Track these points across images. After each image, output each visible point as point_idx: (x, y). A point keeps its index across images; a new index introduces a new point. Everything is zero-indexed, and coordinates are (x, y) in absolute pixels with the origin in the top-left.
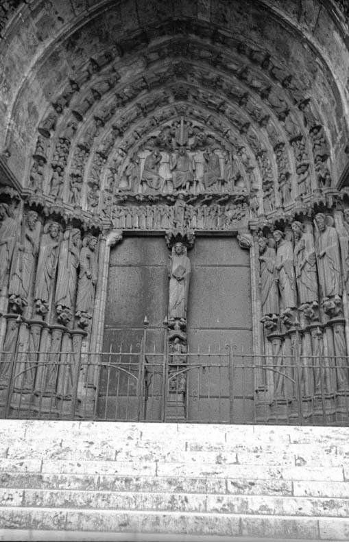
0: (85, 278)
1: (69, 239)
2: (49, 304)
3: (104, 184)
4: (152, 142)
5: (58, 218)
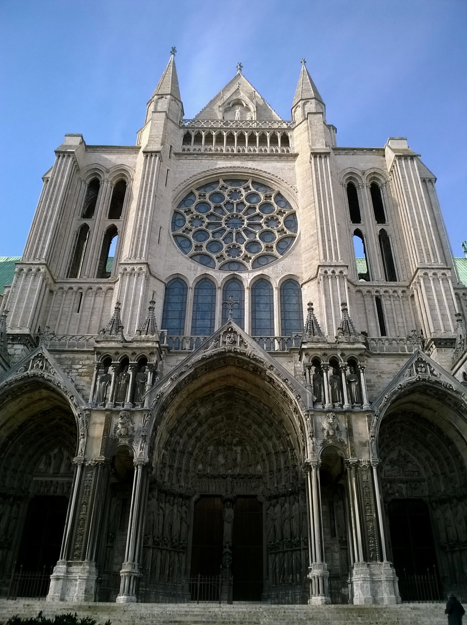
0: (184, 523)
1: (177, 504)
2: (169, 539)
3: (191, 469)
4: (215, 442)
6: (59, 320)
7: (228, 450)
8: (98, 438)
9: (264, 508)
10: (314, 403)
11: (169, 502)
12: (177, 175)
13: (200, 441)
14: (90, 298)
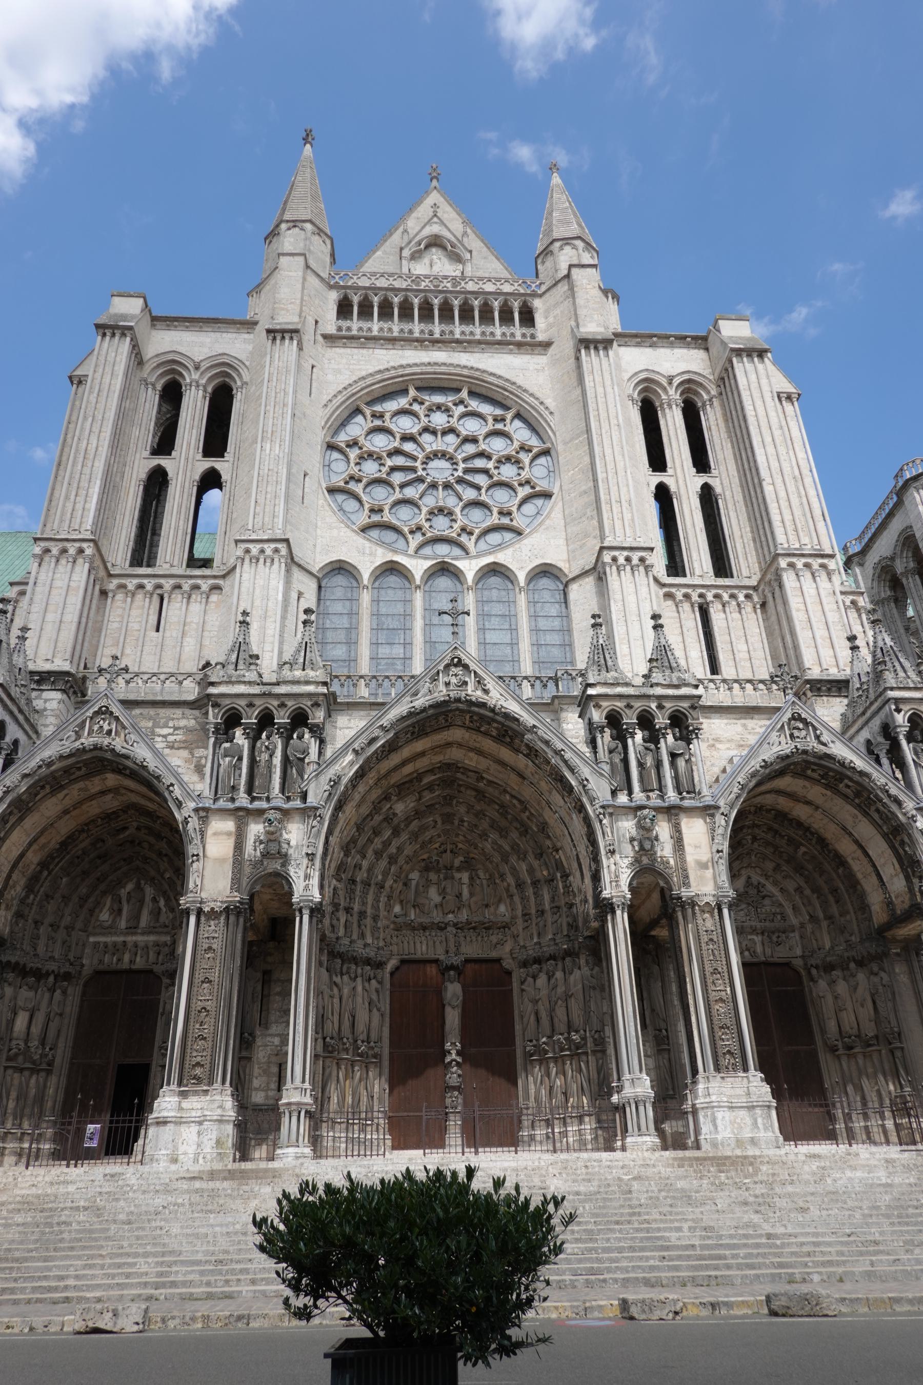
0: (375, 1010)
3: (383, 913)
4: (423, 864)
5: (355, 960)
6: (121, 645)
7: (445, 879)
8: (223, 860)
9: (514, 979)
10: (614, 793)
11: (348, 973)
12: (330, 377)
13: (396, 862)
14: (178, 605)
